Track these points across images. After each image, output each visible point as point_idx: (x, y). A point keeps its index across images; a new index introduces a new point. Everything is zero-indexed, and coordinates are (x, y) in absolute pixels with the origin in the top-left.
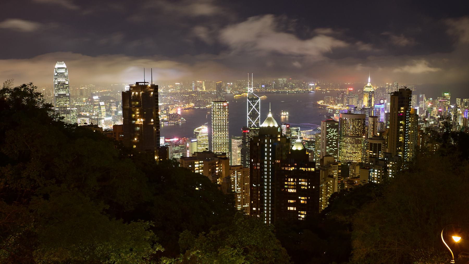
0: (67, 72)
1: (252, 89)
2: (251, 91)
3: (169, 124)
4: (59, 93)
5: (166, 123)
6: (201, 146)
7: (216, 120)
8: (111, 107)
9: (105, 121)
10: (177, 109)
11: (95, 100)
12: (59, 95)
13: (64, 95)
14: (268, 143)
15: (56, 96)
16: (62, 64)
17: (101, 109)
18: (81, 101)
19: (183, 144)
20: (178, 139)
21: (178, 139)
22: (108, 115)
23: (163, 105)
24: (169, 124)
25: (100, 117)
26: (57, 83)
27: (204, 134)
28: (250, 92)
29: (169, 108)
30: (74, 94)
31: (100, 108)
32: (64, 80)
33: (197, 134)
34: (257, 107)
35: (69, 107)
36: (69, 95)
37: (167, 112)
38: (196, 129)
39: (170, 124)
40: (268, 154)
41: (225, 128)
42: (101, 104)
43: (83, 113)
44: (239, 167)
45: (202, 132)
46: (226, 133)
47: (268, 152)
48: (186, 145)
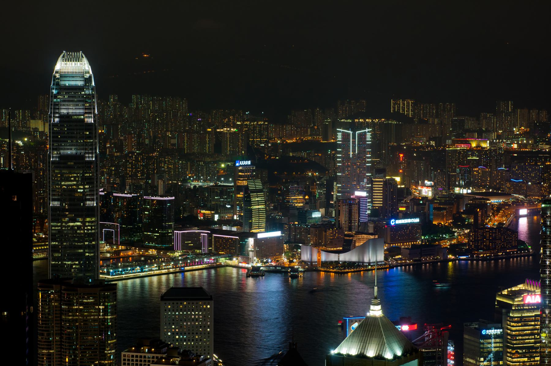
0: (93, 84)
3: (472, 261)
5: (464, 257)
6: (517, 352)
8: (288, 195)
9: (258, 242)
10: (517, 212)
11: (241, 171)
12: (62, 157)
13: (78, 159)
15: (53, 162)
16: (78, 59)
17: (250, 201)
18: (215, 175)
19: (434, 345)
22: (271, 225)
23: (472, 193)
24: (472, 261)
25: (246, 229)
26: (57, 120)
27: (529, 310)
29: (484, 206)
30: (196, 149)
31: (247, 201)
33: (504, 311)
35: (93, 200)
36: (94, 159)
37: (476, 220)
38: (505, 292)
39: (477, 264)
43: (203, 211)
45: (523, 305)
48: (443, 350)
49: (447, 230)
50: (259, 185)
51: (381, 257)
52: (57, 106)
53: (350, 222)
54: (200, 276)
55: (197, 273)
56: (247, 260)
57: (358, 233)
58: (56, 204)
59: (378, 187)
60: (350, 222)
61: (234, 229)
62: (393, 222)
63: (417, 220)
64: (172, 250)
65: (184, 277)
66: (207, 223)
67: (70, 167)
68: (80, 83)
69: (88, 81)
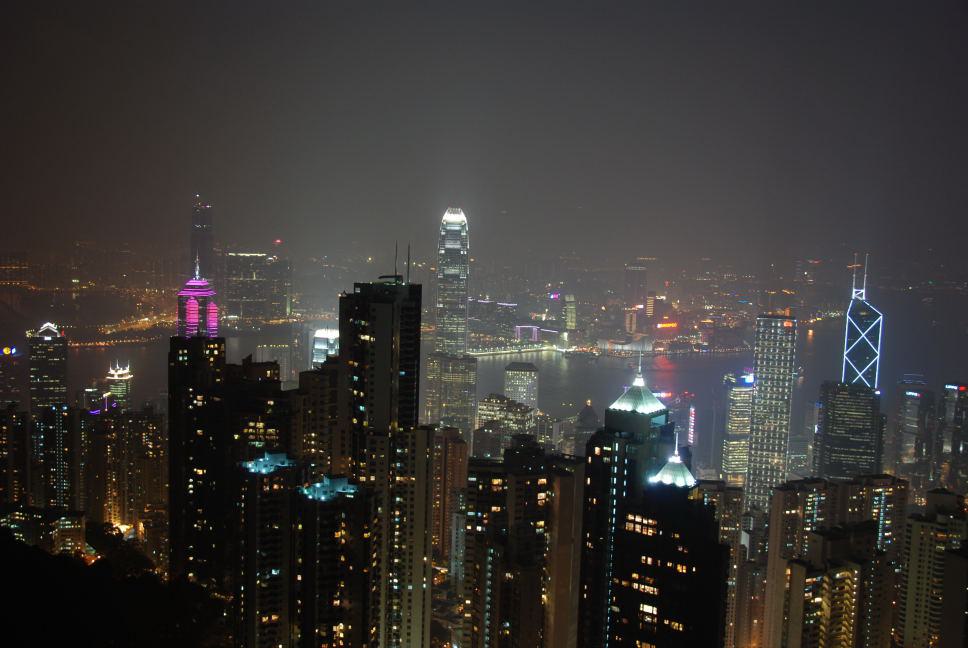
1: (863, 291)
2: (861, 295)
4: (448, 272)
7: (762, 359)
12: (447, 276)
13: (456, 277)
14: (622, 454)
20: (670, 395)
21: (670, 395)
28: (859, 298)
32: (458, 246)
34: (873, 335)
40: (620, 482)
41: (784, 380)
42: (567, 299)
44: (715, 487)
46: (783, 391)
47: (620, 476)
49: (695, 332)
50: (572, 299)
51: (651, 349)
52: (443, 243)
53: (631, 324)
54: (532, 356)
55: (529, 354)
56: (562, 346)
57: (637, 331)
58: (441, 306)
59: (650, 302)
60: (631, 324)
61: (555, 326)
62: (659, 326)
63: (674, 325)
64: (514, 338)
65: (521, 357)
66: (538, 322)
67: (451, 282)
68: (457, 228)
69: (463, 227)
